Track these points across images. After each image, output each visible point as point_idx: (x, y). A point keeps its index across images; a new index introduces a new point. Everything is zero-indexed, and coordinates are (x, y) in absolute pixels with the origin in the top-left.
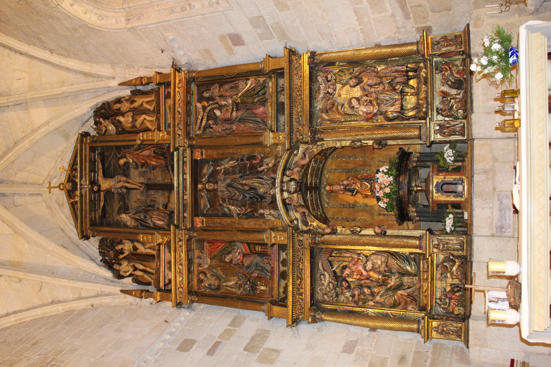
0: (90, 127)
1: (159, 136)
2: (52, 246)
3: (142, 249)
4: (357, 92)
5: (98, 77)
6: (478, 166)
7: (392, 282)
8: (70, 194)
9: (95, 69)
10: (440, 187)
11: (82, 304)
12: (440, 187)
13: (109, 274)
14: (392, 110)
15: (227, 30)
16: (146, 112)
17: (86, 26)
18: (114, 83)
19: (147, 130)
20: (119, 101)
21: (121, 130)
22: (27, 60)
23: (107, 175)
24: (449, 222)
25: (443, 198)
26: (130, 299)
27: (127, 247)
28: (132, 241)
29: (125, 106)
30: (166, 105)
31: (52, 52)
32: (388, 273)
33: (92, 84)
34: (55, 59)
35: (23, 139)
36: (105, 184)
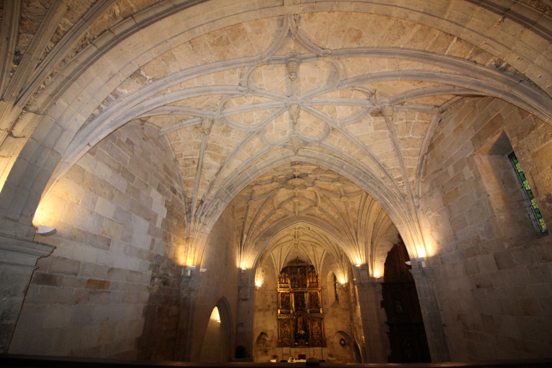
0: (310, 264)
1: (308, 285)
2: (285, 256)
3: (286, 279)
4: (317, 326)
5: (319, 267)
6: (305, 349)
7: (286, 333)
8: (296, 261)
9: (321, 267)
10: (302, 342)
11: (275, 266)
12: (302, 342)
13: (281, 270)
14: (314, 332)
15: (327, 303)
16: (313, 280)
17: (327, 273)
18: (318, 272)
19: (309, 280)
20: (315, 272)
21: (309, 272)
22: (322, 252)
23: (300, 270)
24: (296, 344)
25: (300, 342)
26: (277, 276)
27: (287, 275)
28: (288, 277)
29: (314, 274)
30: (314, 284)
31: (324, 259)
32: (287, 332)
33: (318, 266)
34: (323, 259)
35: (307, 249)
36: (298, 270)
